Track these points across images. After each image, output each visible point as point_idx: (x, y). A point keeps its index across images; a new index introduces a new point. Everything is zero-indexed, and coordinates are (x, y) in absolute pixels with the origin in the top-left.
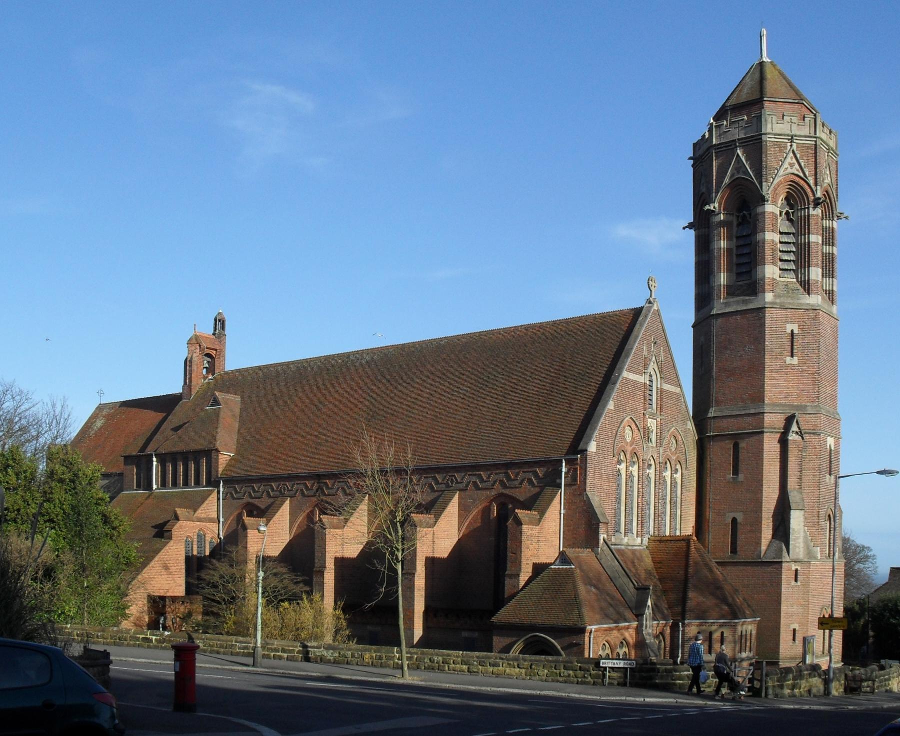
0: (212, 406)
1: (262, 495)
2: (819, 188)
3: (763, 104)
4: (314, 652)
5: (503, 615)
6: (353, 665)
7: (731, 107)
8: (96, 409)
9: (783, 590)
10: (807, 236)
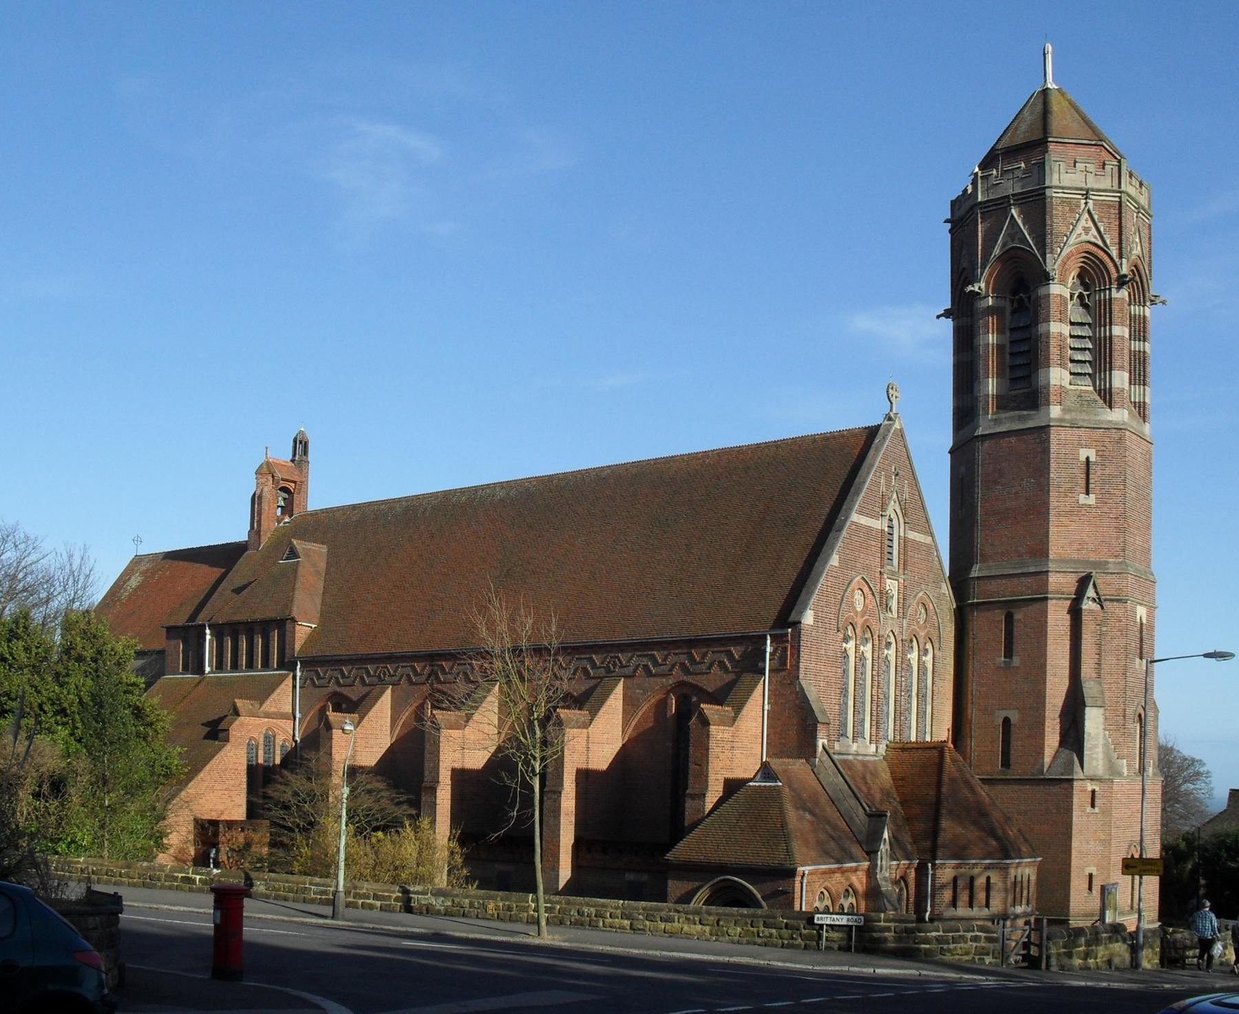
0: (287, 559)
1: (354, 682)
2: (1124, 261)
3: (1047, 147)
4: (418, 900)
5: (682, 851)
6: (471, 917)
7: (1003, 151)
8: (131, 562)
9: (1074, 819)
10: (1108, 327)
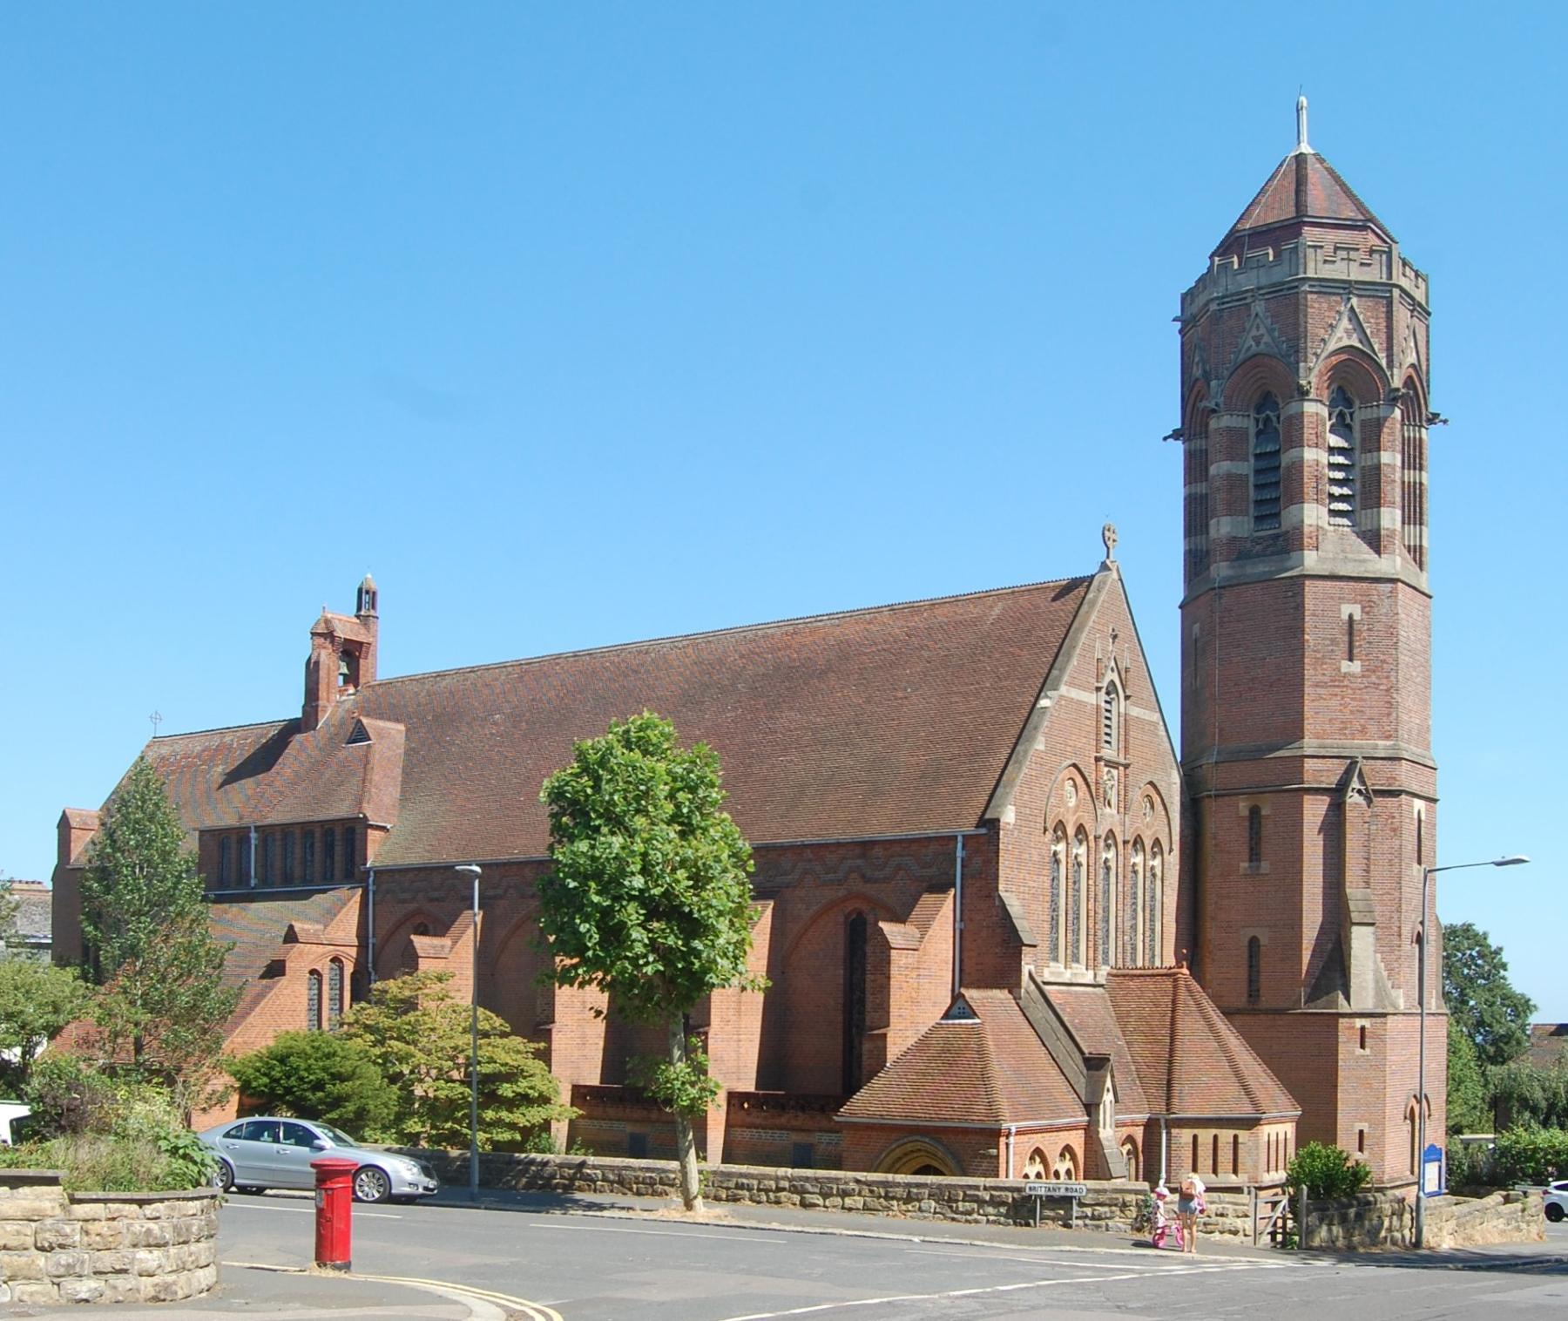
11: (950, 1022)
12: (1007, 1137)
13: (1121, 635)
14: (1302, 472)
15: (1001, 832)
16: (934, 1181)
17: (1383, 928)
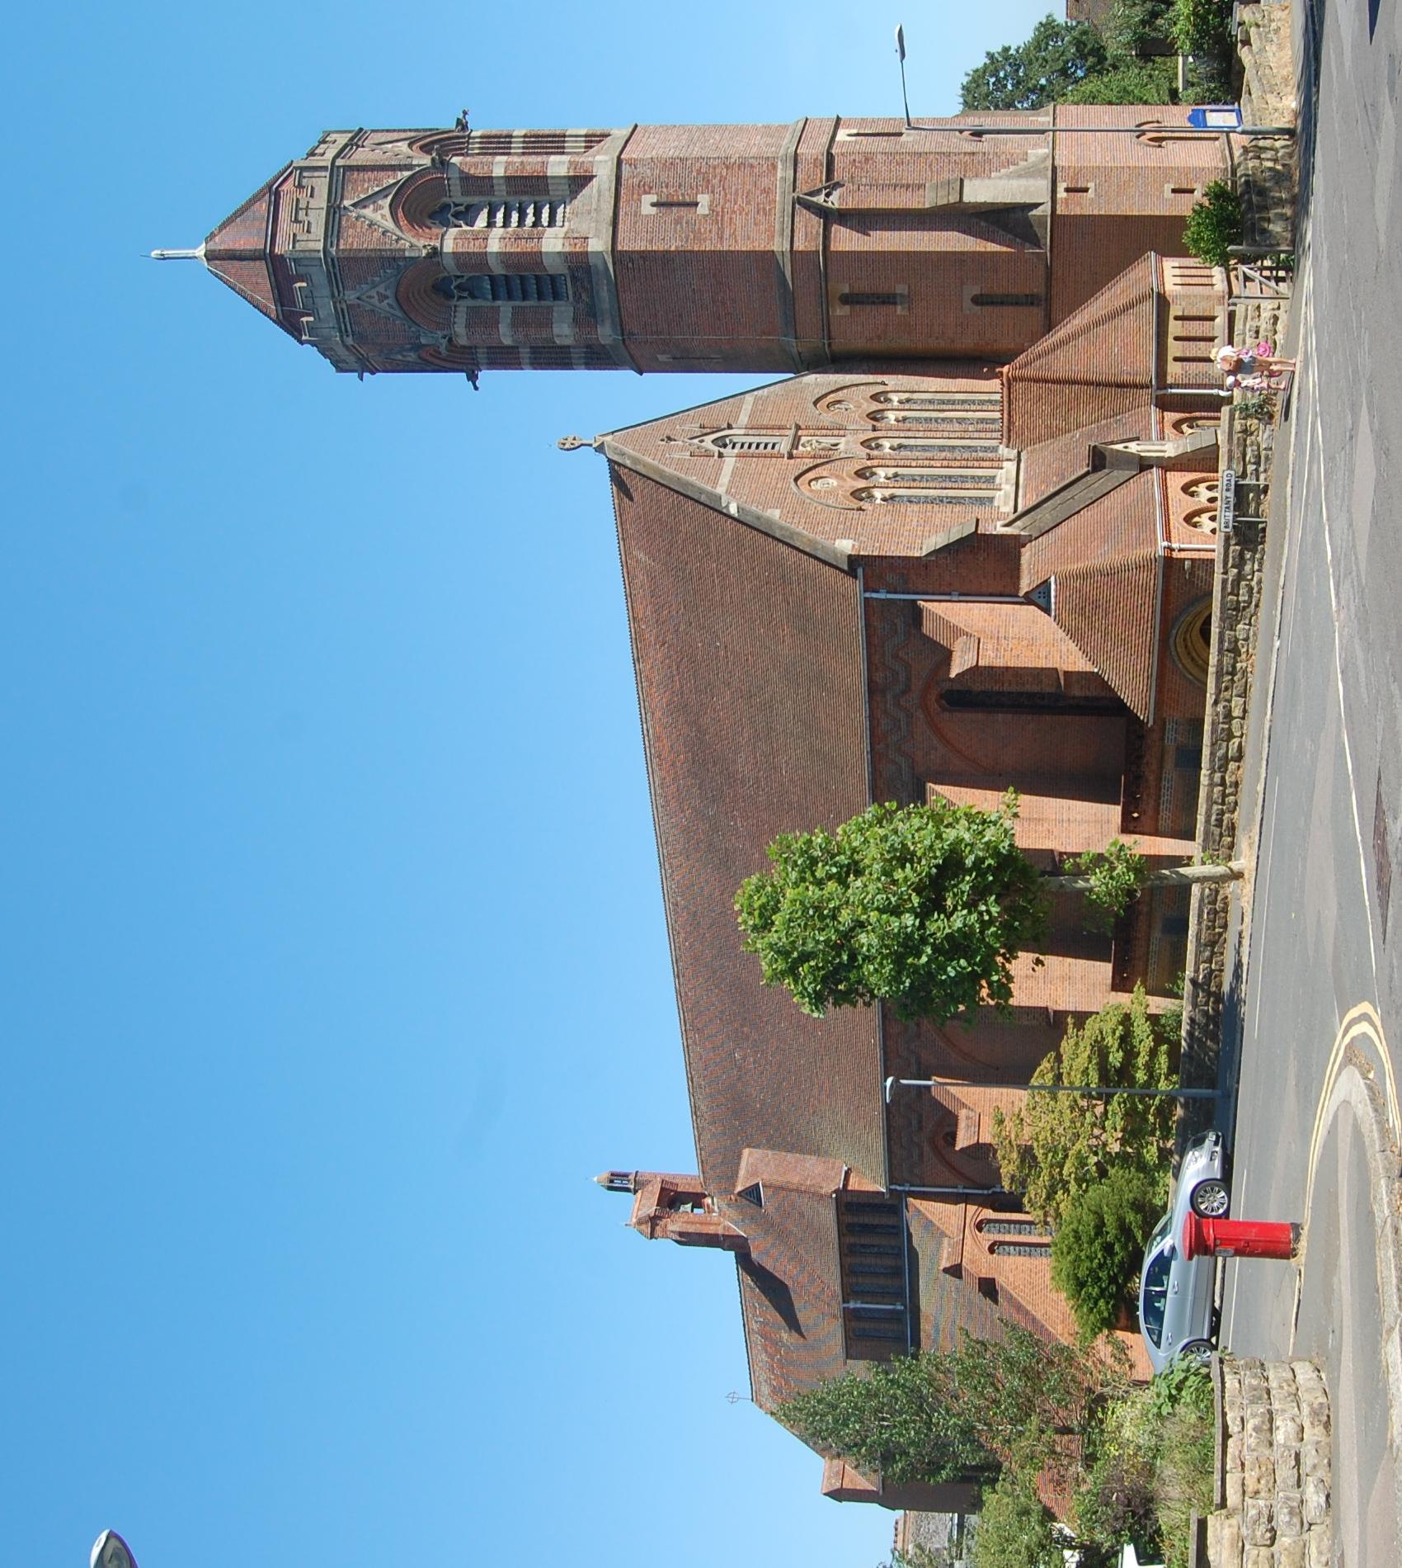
2: (415, 162)
11: (1053, 607)
12: (1172, 550)
13: (668, 432)
14: (511, 254)
15: (862, 553)
16: (1217, 625)
17: (965, 171)
